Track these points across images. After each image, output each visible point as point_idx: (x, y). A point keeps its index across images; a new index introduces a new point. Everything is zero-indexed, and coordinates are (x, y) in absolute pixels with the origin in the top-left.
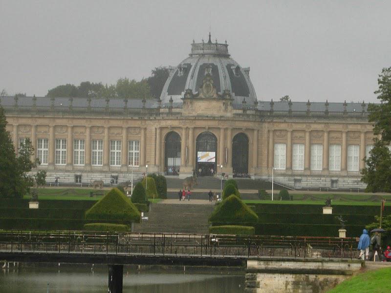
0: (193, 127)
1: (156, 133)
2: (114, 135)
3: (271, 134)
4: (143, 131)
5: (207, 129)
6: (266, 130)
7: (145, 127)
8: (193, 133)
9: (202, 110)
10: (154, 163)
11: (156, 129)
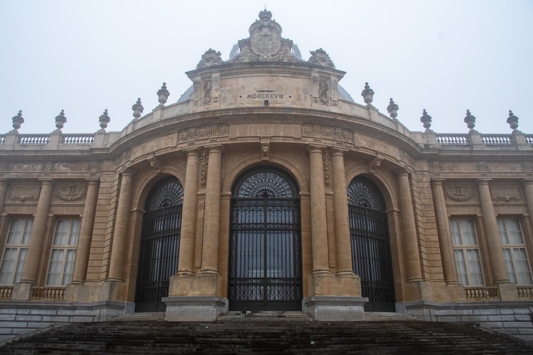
0: (219, 143)
1: (119, 190)
2: (18, 202)
3: (440, 189)
4: (90, 189)
5: (265, 149)
6: (426, 179)
7: (95, 178)
8: (223, 165)
9: (249, 96)
10: (103, 276)
11: (121, 175)
